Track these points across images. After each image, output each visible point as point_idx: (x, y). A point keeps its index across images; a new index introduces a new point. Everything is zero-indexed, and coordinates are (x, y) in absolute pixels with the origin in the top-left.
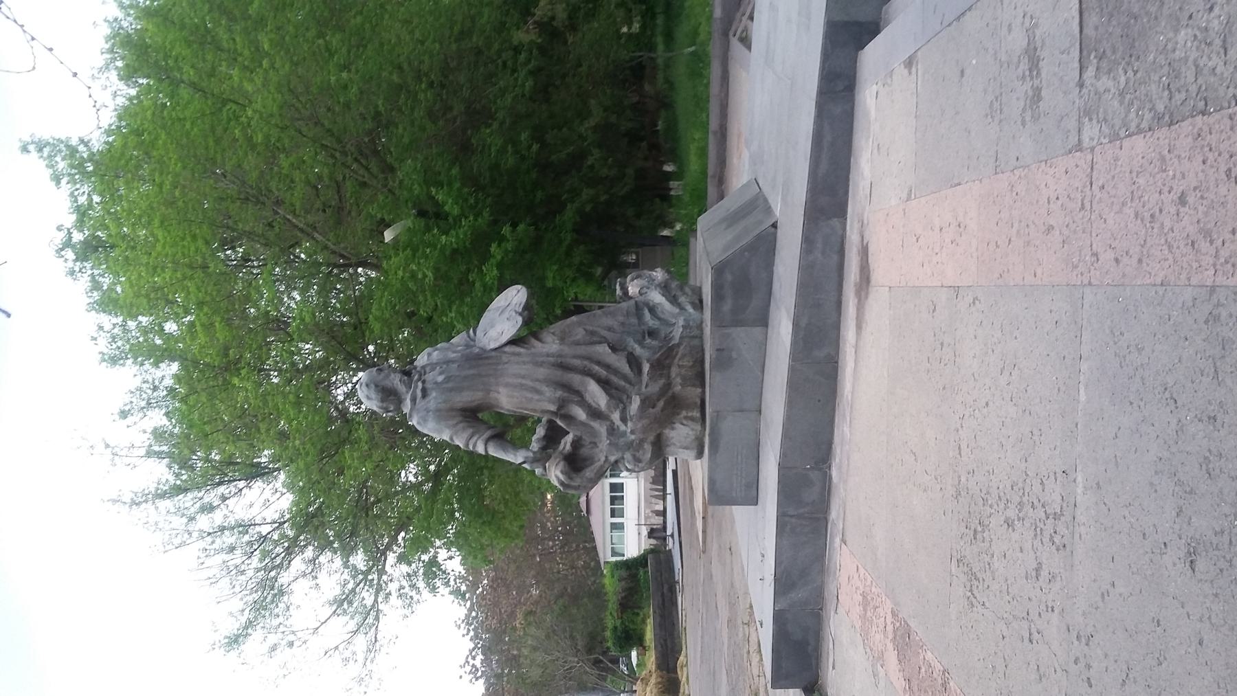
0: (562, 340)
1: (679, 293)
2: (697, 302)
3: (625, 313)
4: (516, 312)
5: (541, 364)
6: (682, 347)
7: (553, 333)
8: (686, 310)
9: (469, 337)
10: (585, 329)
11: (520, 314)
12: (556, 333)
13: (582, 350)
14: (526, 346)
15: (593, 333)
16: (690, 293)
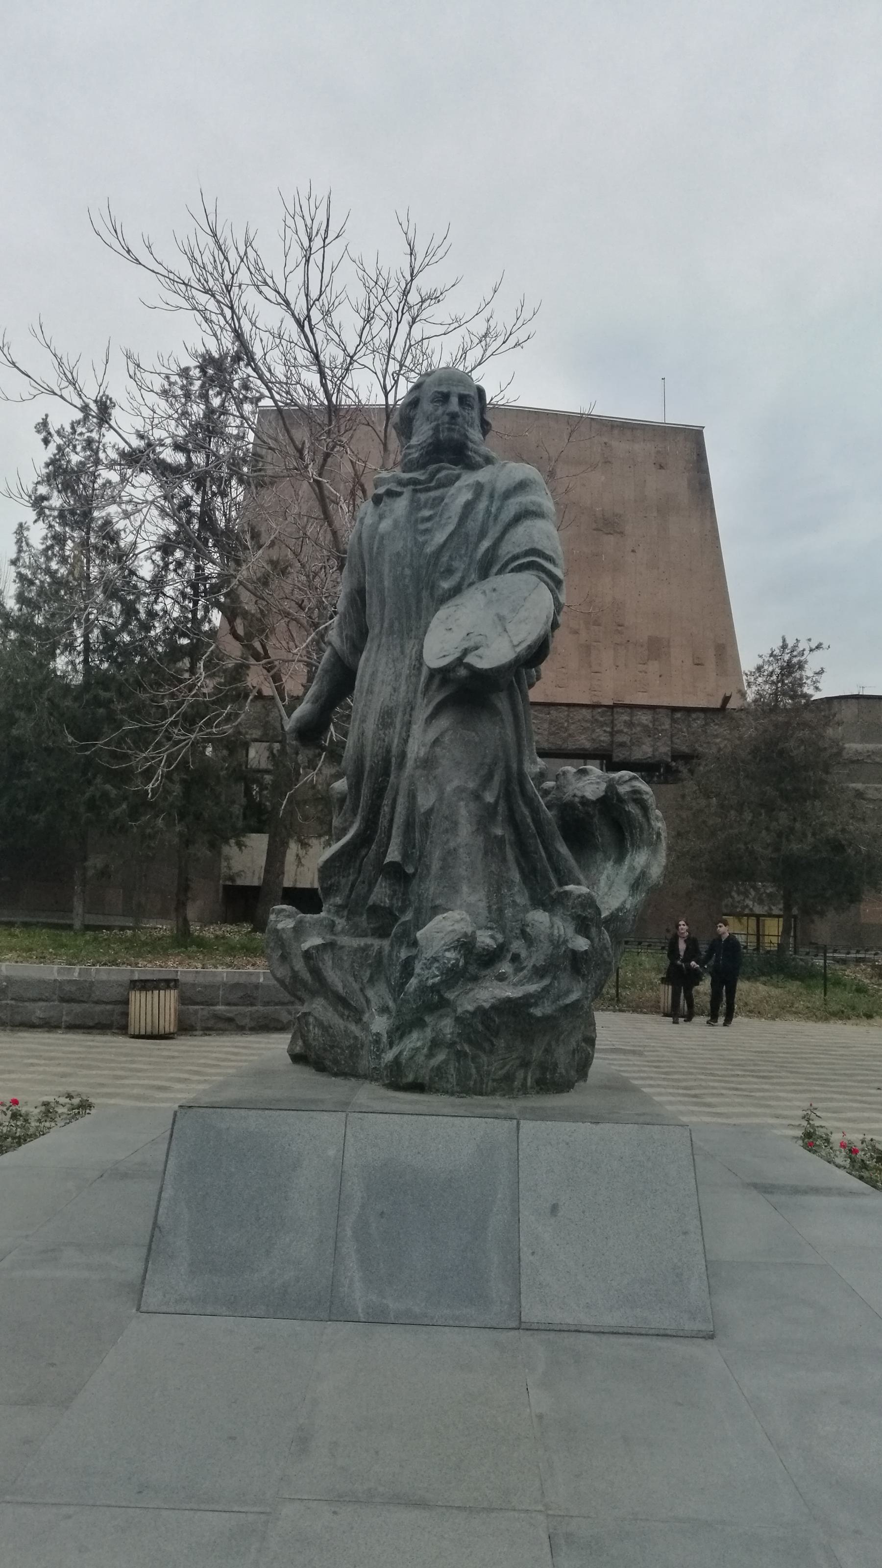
0: (428, 763)
1: (429, 1033)
2: (410, 1078)
3: (437, 902)
4: (466, 652)
5: (386, 718)
6: (353, 1027)
7: (436, 742)
8: (391, 1048)
9: (515, 558)
10: (430, 811)
11: (459, 661)
12: (438, 750)
13: (400, 809)
14: (434, 687)
15: (425, 826)
16: (435, 1062)
